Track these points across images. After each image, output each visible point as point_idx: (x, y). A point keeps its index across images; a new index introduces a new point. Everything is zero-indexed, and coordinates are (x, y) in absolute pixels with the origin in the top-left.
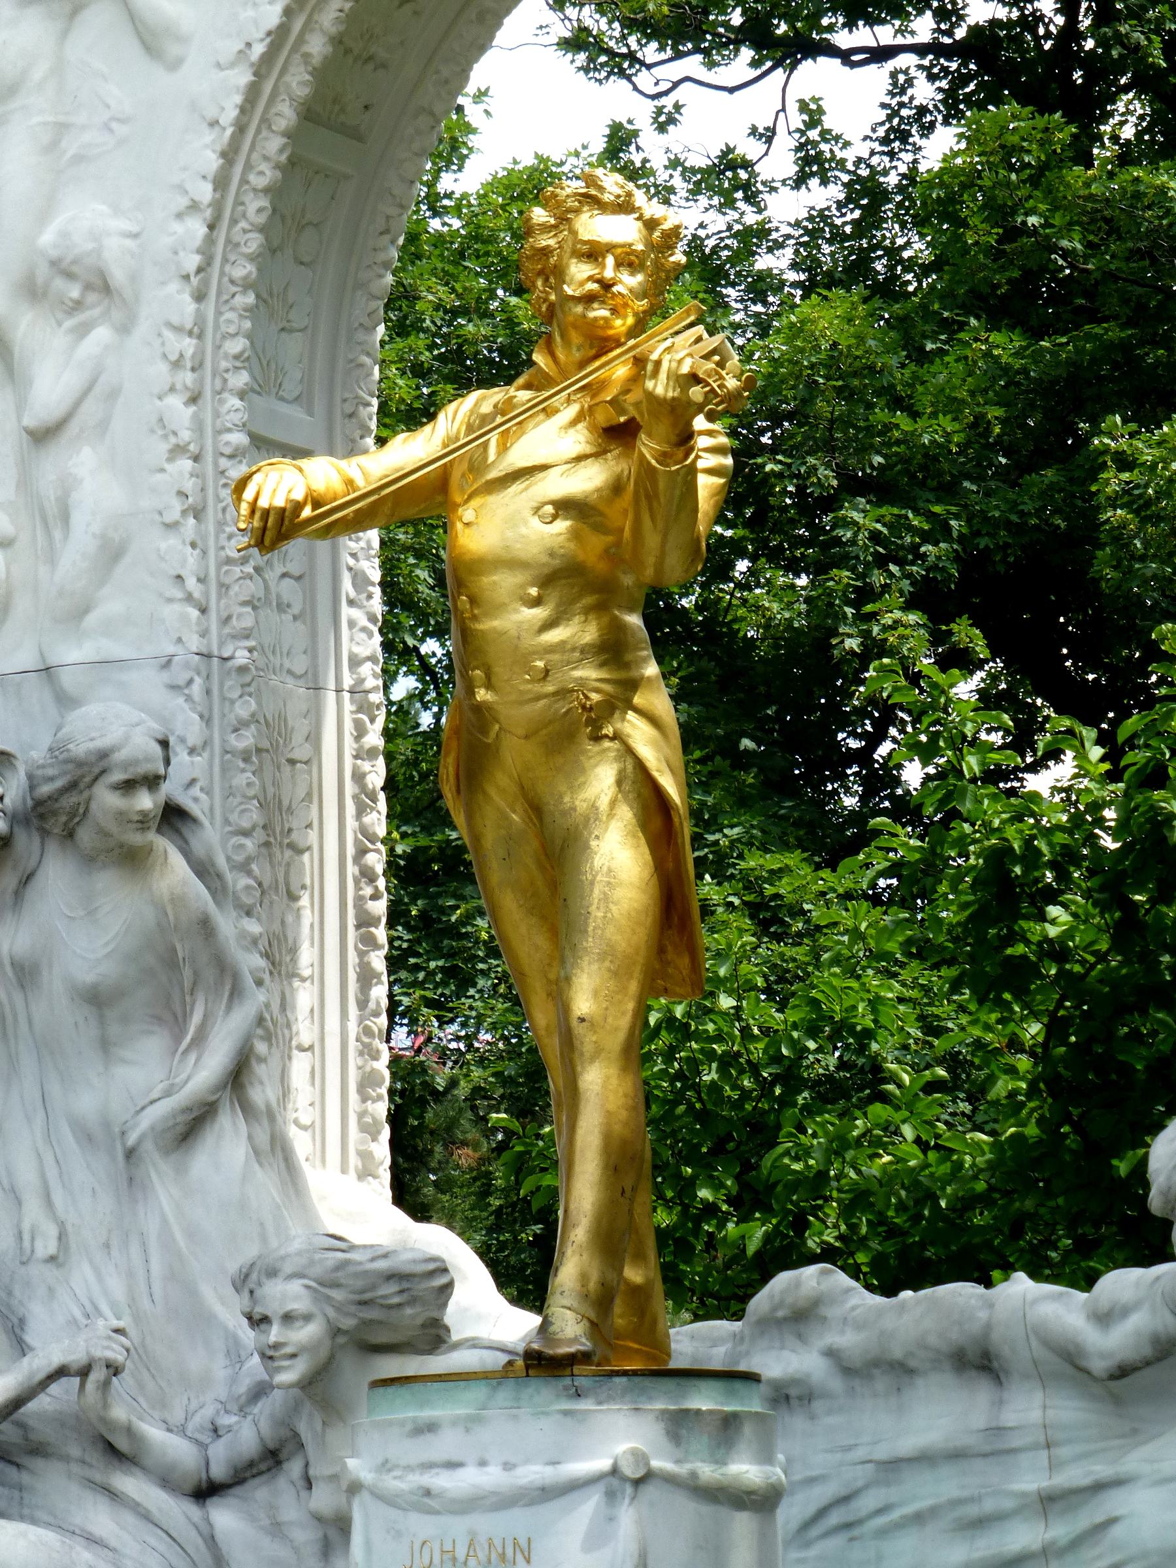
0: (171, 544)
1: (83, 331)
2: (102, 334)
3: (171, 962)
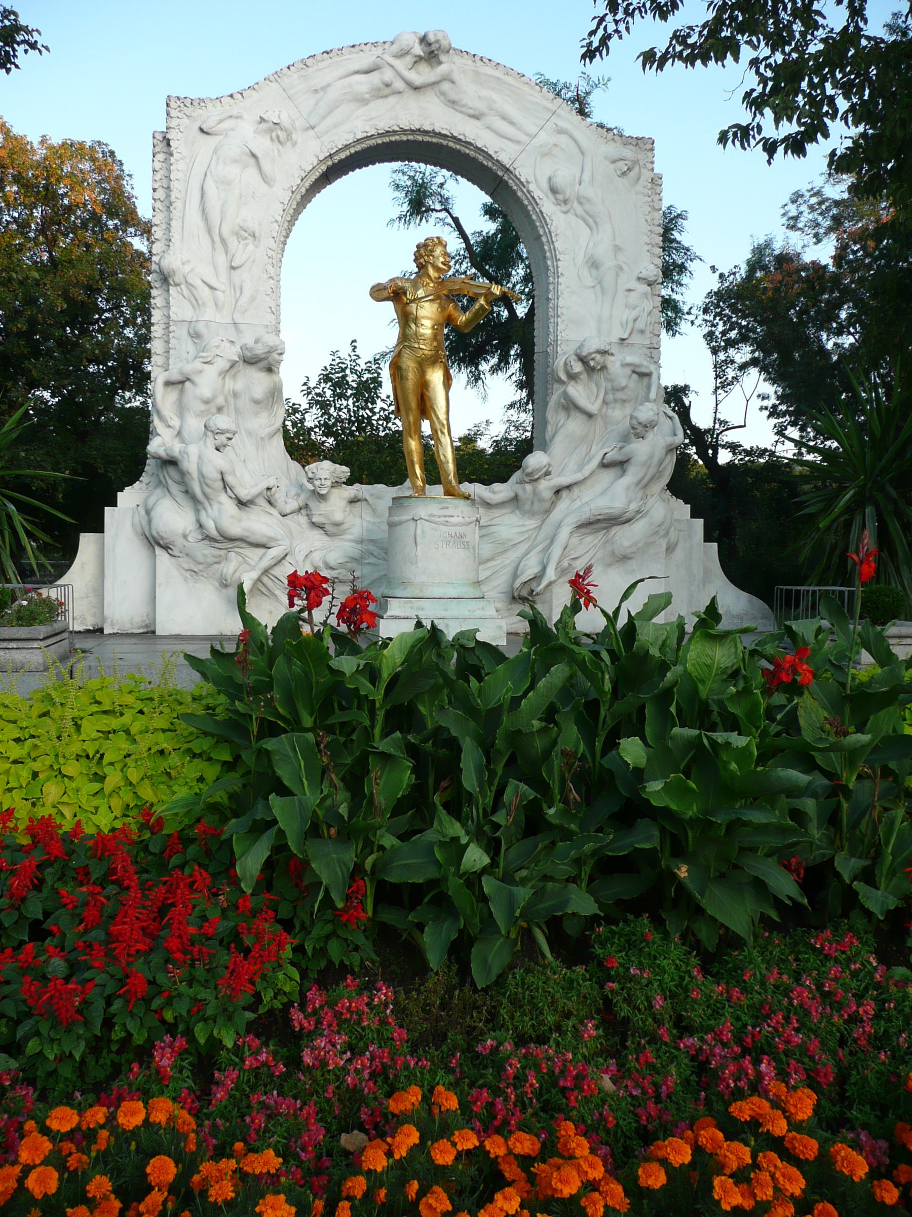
0: (267, 298)
1: (247, 245)
2: (251, 247)
3: (273, 395)
